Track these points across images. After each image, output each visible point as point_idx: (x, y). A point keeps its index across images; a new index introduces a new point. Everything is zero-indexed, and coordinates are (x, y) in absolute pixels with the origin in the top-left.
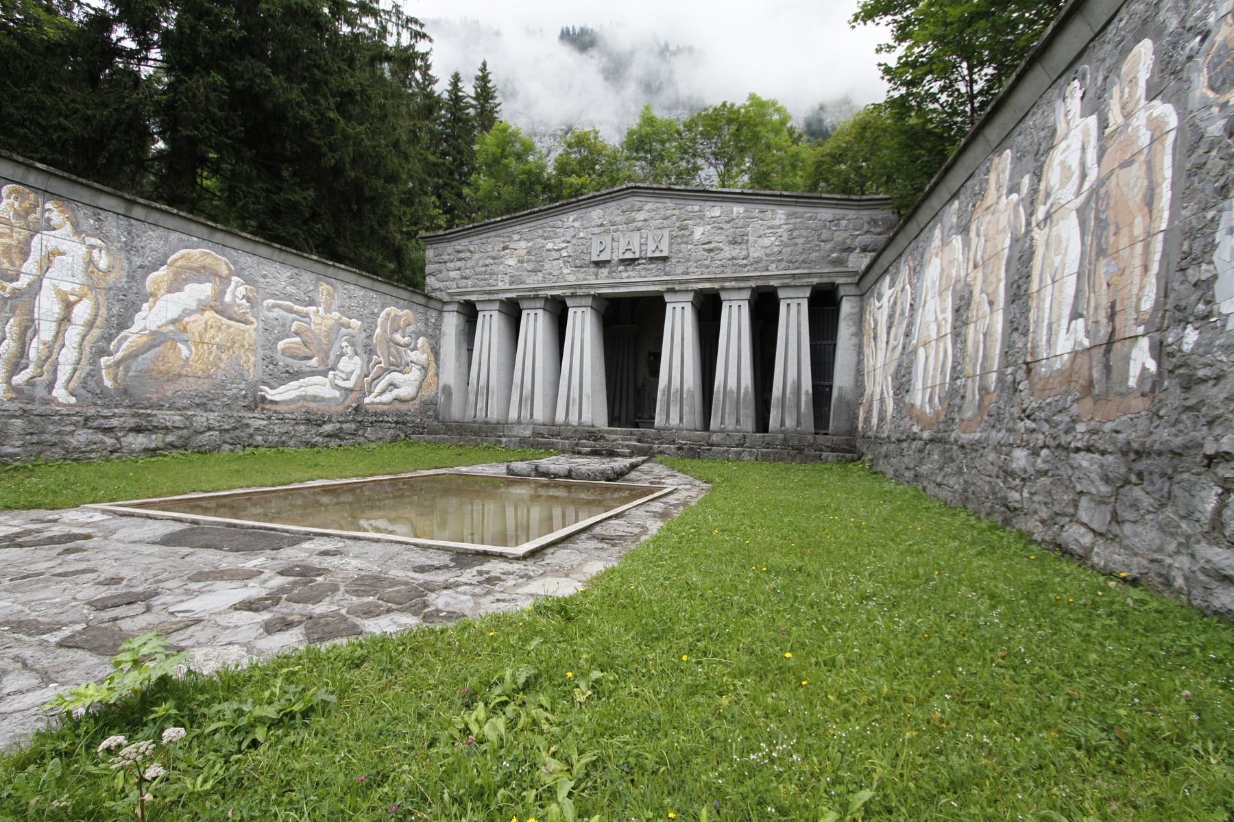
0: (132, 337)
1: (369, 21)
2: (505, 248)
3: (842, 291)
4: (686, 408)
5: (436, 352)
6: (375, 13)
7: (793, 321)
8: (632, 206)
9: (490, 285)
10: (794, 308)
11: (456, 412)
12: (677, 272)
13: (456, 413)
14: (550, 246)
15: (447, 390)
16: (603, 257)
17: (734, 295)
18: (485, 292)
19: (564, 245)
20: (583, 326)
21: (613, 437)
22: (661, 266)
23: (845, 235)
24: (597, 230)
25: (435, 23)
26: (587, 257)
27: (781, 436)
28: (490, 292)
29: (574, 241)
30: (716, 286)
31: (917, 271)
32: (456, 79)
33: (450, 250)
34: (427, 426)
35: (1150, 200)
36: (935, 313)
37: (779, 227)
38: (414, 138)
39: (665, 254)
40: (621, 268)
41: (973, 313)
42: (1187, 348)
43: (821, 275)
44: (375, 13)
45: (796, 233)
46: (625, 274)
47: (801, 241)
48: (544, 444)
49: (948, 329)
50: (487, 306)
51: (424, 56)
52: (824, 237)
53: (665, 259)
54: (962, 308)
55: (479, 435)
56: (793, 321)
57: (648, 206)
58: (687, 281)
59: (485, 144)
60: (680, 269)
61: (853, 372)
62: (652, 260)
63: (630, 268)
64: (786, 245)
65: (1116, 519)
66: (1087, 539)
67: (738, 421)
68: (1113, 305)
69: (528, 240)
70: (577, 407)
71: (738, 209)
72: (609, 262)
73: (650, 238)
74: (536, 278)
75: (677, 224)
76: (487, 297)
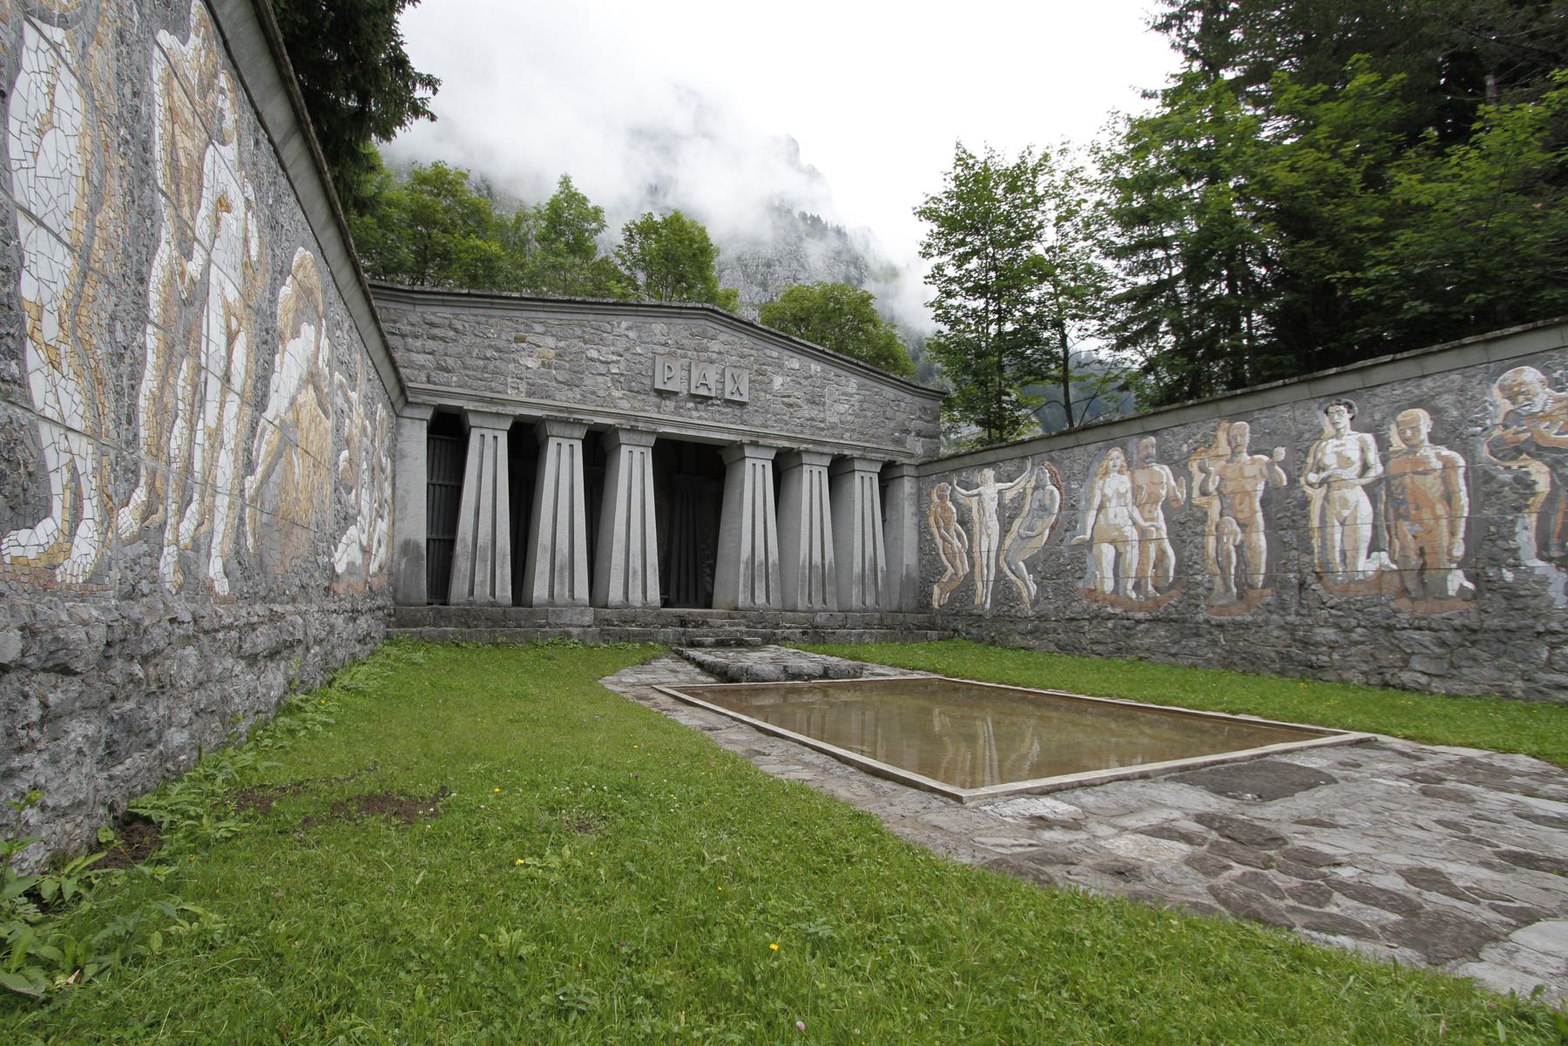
2: (519, 340)
4: (772, 585)
8: (704, 332)
9: (492, 390)
10: (867, 481)
12: (755, 423)
14: (593, 354)
16: (669, 387)
17: (816, 460)
18: (482, 399)
19: (615, 358)
20: (634, 474)
21: (719, 622)
22: (737, 412)
23: (904, 416)
24: (660, 350)
26: (647, 382)
27: (877, 615)
28: (492, 401)
29: (628, 355)
30: (803, 446)
33: (414, 318)
35: (1449, 498)
37: (852, 395)
39: (745, 399)
40: (690, 405)
43: (886, 452)
45: (865, 405)
46: (695, 414)
47: (870, 414)
48: (636, 635)
50: (489, 422)
52: (889, 414)
53: (742, 404)
57: (723, 337)
58: (766, 436)
60: (758, 420)
61: (915, 550)
62: (729, 402)
63: (701, 407)
64: (857, 416)
65: (1452, 665)
66: (1424, 680)
67: (824, 601)
68: (1421, 549)
69: (559, 339)
70: (639, 582)
71: (816, 367)
72: (676, 393)
73: (728, 376)
74: (570, 394)
75: (756, 367)
76: (494, 409)
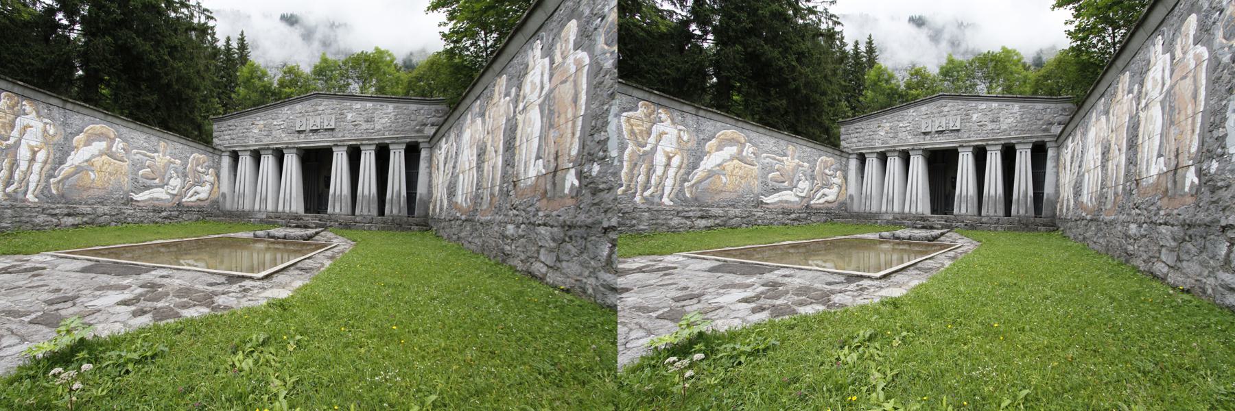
0: (66, 168)
1: (185, 10)
3: (421, 146)
5: (218, 176)
6: (187, 7)
7: (397, 160)
11: (228, 206)
13: (228, 206)
15: (224, 195)
25: (218, 11)
31: (459, 136)
32: (228, 39)
34: (214, 213)
36: (468, 157)
38: (207, 69)
41: (487, 157)
42: (594, 174)
44: (187, 7)
49: (474, 164)
51: (212, 28)
54: (481, 154)
55: (240, 218)
56: (397, 160)
59: (243, 72)
